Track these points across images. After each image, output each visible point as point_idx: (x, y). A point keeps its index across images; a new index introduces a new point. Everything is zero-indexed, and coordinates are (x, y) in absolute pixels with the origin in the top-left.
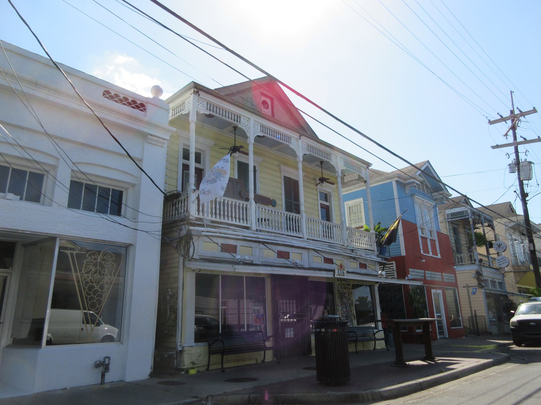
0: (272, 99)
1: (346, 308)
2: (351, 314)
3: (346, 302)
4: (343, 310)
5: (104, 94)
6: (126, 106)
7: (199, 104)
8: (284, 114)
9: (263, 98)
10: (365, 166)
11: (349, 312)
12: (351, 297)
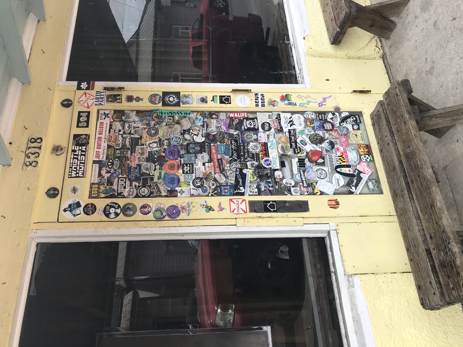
1: (196, 153)
2: (222, 116)
3: (160, 143)
4: (207, 177)
11: (213, 128)
12: (134, 105)
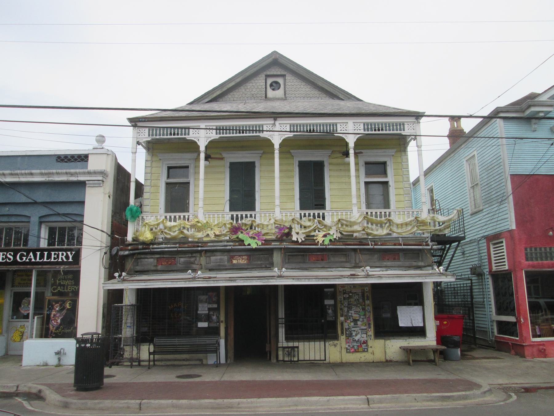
0: (283, 76)
5: (57, 160)
6: (73, 163)
7: (139, 134)
8: (302, 86)
9: (270, 81)
10: (413, 119)
